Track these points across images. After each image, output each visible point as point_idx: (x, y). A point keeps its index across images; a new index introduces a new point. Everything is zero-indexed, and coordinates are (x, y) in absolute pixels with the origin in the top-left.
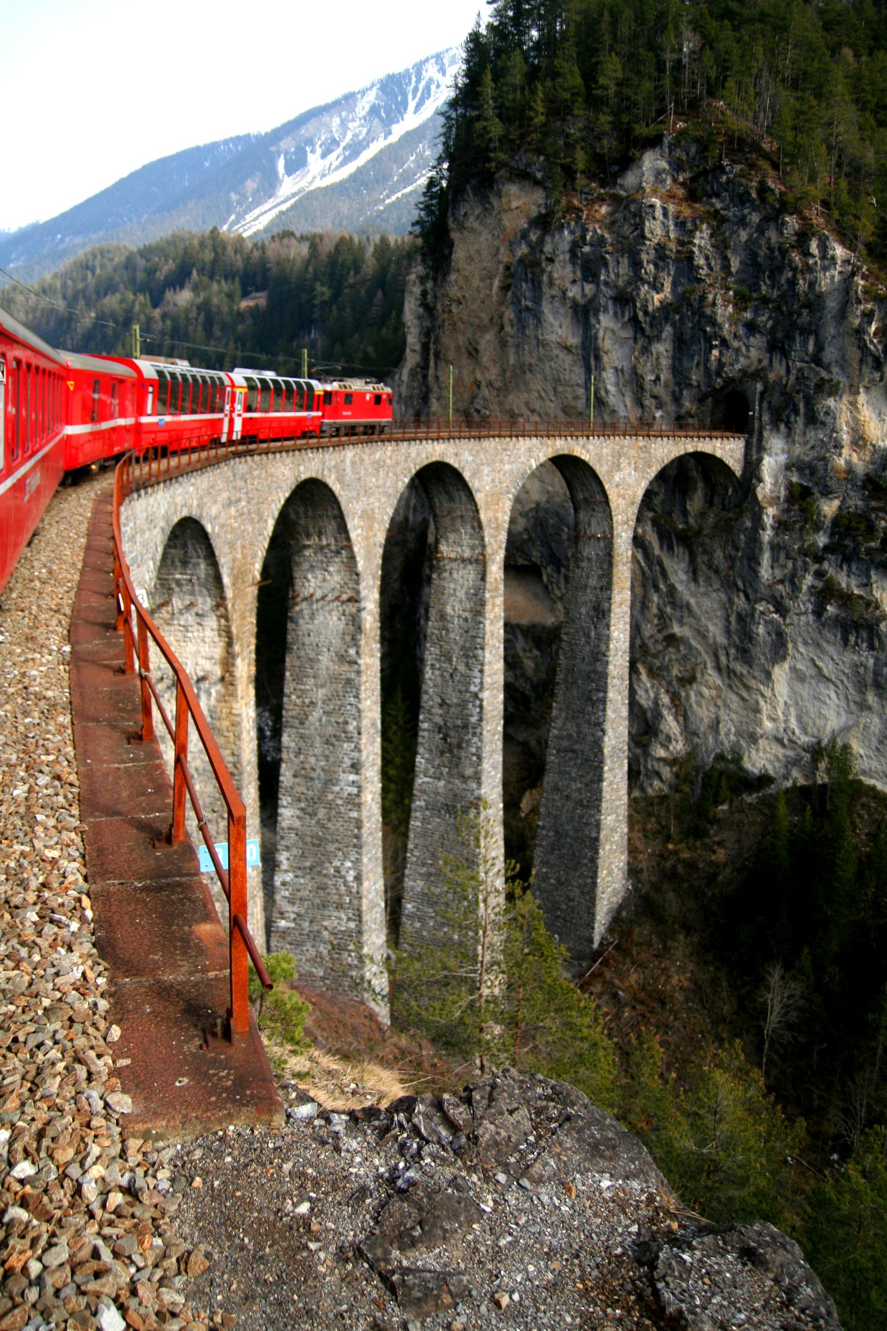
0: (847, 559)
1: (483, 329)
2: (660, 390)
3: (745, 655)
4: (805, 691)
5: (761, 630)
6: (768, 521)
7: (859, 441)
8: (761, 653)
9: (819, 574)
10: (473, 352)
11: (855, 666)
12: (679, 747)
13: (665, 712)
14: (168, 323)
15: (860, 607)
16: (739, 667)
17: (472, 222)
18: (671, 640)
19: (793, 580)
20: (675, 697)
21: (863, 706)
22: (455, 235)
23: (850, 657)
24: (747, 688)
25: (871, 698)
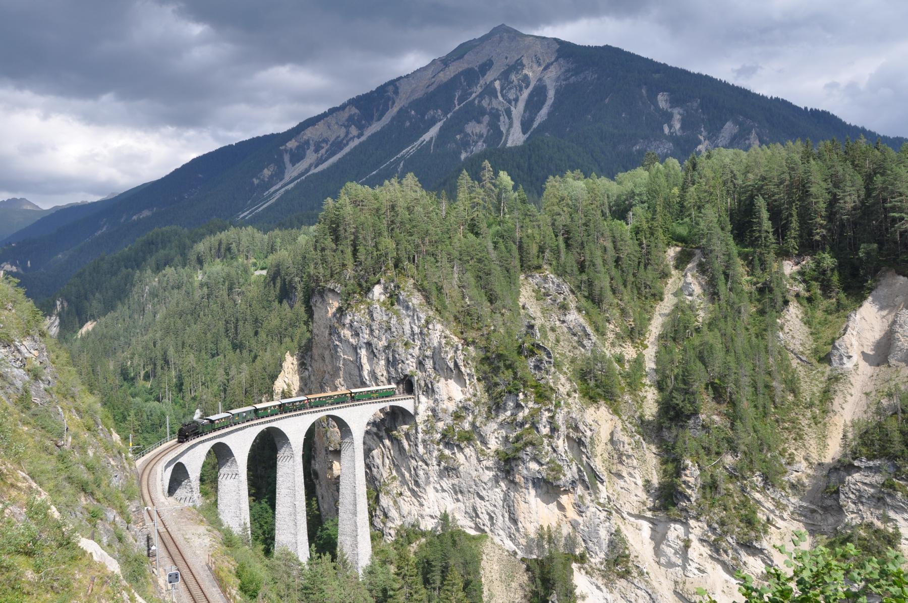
0: (448, 445)
1: (325, 349)
2: (383, 379)
3: (417, 483)
4: (439, 495)
5: (421, 473)
6: (420, 430)
7: (450, 399)
8: (422, 480)
9: (439, 450)
10: (323, 359)
11: (453, 485)
12: (398, 523)
13: (391, 508)
14: (205, 289)
15: (452, 461)
16: (416, 489)
17: (318, 304)
18: (394, 478)
19: (430, 452)
20: (395, 502)
21: (458, 500)
22: (314, 308)
23: (451, 481)
24: (420, 497)
25: (460, 496)
